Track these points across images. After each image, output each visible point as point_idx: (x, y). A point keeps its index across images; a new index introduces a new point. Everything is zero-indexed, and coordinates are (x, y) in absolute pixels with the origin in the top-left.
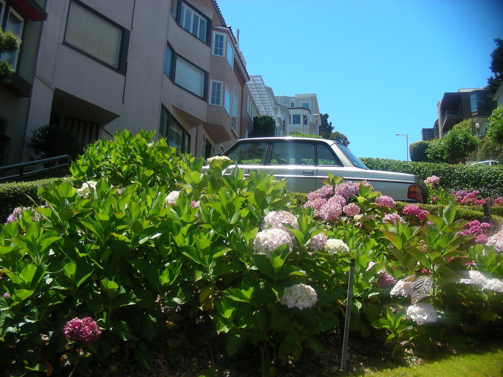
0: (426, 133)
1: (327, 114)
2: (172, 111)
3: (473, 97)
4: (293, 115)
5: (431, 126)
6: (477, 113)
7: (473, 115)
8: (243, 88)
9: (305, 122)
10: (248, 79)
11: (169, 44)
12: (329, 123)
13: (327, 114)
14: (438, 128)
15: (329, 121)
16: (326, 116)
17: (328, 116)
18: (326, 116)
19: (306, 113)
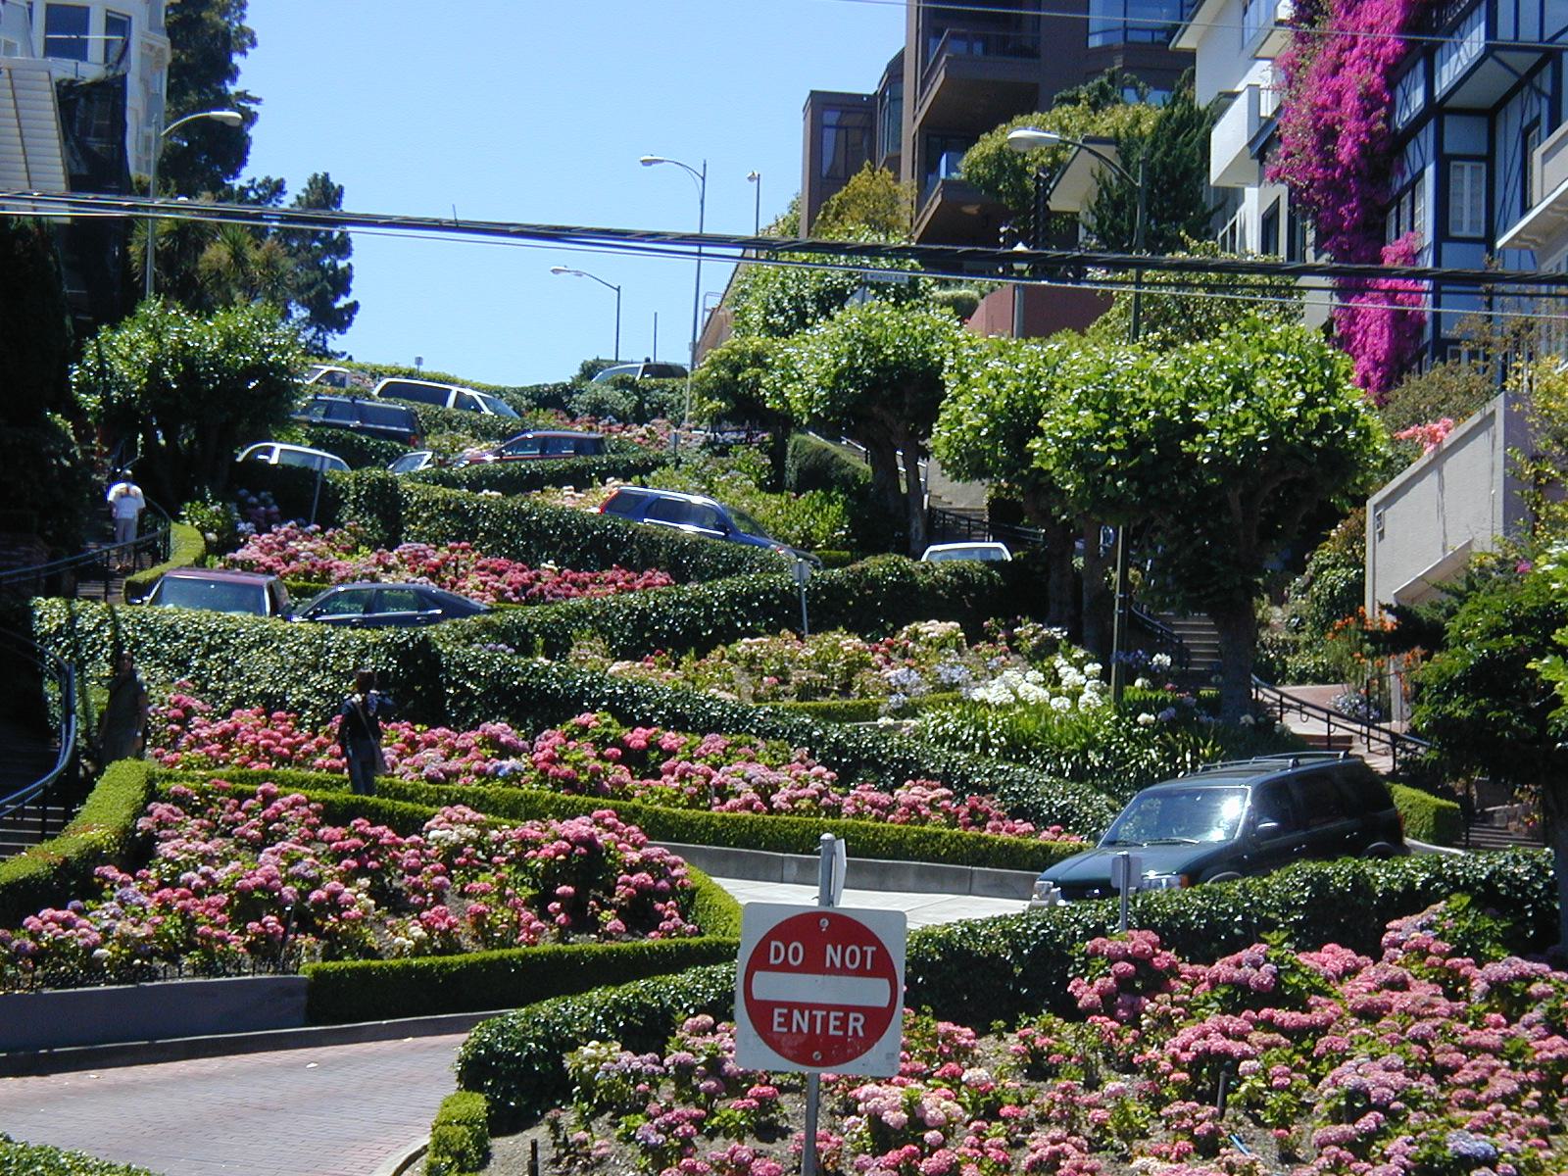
0: (831, 117)
4: (49, 7)
5: (866, 82)
14: (898, 99)
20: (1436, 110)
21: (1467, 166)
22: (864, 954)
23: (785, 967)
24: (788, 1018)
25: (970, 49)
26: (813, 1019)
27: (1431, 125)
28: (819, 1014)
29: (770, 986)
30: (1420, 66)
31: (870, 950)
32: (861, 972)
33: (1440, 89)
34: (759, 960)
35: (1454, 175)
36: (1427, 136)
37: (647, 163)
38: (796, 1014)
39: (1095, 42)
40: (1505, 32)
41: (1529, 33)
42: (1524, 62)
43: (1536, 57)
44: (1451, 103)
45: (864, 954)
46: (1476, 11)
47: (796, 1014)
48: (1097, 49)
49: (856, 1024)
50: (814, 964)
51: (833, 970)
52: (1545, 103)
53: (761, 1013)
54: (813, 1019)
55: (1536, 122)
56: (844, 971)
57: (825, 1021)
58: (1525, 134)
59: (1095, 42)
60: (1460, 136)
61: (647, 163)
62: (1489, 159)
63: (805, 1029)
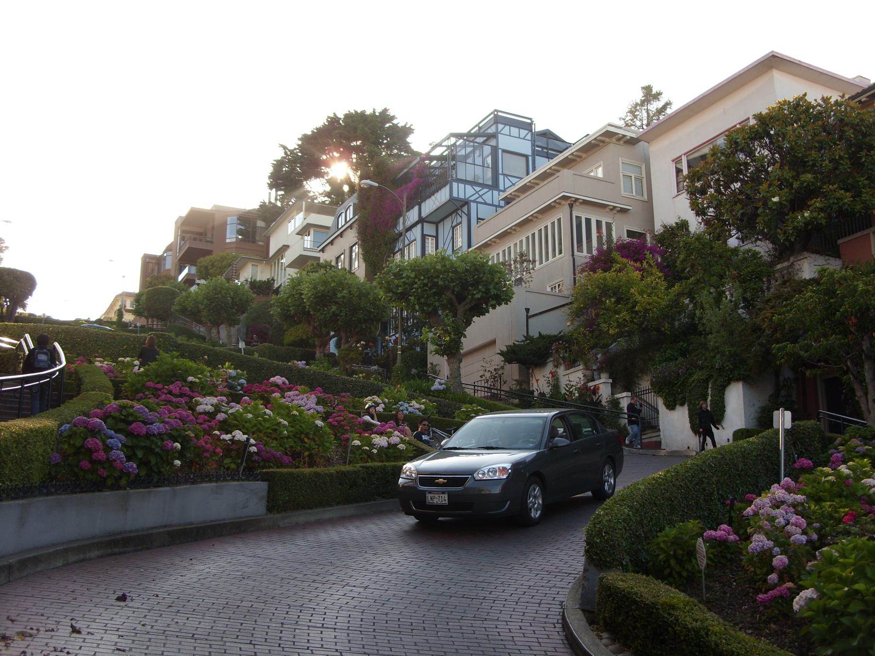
5: (158, 252)
20: (421, 221)
21: (430, 238)
27: (419, 226)
33: (424, 214)
35: (426, 241)
37: (111, 261)
41: (462, 196)
42: (459, 204)
43: (462, 203)
44: (426, 220)
46: (443, 190)
52: (465, 218)
55: (461, 223)
58: (453, 228)
59: (228, 241)
60: (429, 229)
61: (111, 261)
62: (437, 237)
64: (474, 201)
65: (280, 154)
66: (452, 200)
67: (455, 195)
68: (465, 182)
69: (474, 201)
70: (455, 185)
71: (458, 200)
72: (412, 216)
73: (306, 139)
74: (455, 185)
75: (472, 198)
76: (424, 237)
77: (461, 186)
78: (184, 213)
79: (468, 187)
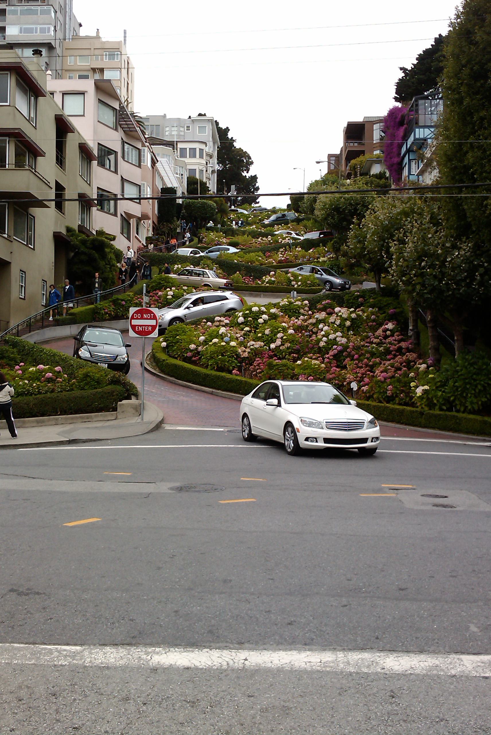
1: (227, 128)
2: (124, 215)
3: (376, 127)
6: (378, 145)
7: (375, 146)
8: (153, 168)
9: (201, 157)
10: (156, 161)
11: (122, 177)
12: (230, 138)
13: (227, 128)
15: (230, 136)
16: (227, 130)
17: (229, 130)
18: (227, 130)
19: (203, 146)
20: (408, 151)
22: (151, 316)
23: (137, 319)
24: (138, 328)
25: (354, 144)
26: (143, 328)
28: (144, 327)
29: (135, 322)
30: (405, 144)
31: (152, 315)
32: (150, 319)
34: (133, 318)
35: (411, 163)
36: (407, 156)
37: (294, 169)
38: (140, 327)
39: (374, 142)
40: (417, 137)
41: (422, 136)
44: (411, 149)
45: (151, 316)
47: (140, 327)
48: (375, 144)
49: (150, 328)
50: (142, 318)
51: (145, 319)
53: (133, 327)
54: (143, 328)
56: (147, 319)
57: (145, 328)
59: (374, 142)
61: (294, 169)
63: (141, 330)
64: (430, 138)
65: (401, 75)
66: (415, 139)
67: (417, 137)
68: (424, 127)
69: (430, 138)
70: (417, 130)
71: (419, 139)
72: (404, 149)
73: (421, 58)
74: (417, 130)
75: (428, 137)
76: (410, 160)
77: (421, 130)
78: (346, 125)
79: (426, 130)
